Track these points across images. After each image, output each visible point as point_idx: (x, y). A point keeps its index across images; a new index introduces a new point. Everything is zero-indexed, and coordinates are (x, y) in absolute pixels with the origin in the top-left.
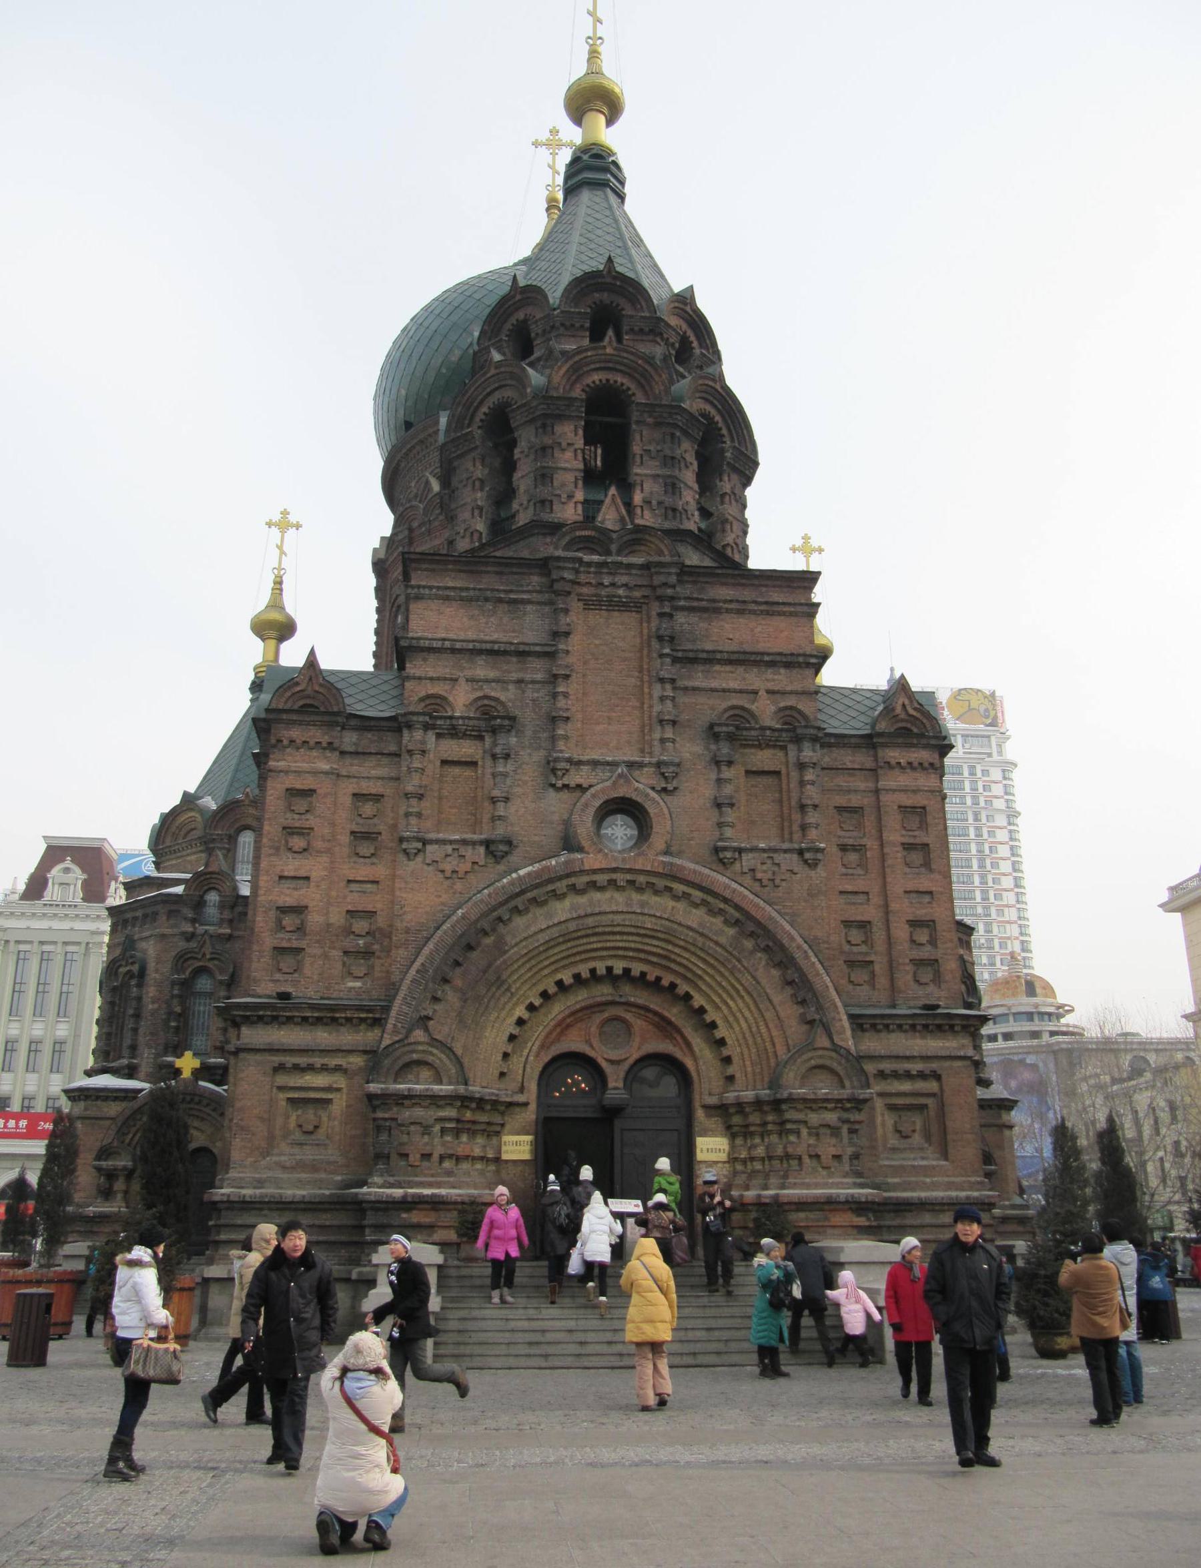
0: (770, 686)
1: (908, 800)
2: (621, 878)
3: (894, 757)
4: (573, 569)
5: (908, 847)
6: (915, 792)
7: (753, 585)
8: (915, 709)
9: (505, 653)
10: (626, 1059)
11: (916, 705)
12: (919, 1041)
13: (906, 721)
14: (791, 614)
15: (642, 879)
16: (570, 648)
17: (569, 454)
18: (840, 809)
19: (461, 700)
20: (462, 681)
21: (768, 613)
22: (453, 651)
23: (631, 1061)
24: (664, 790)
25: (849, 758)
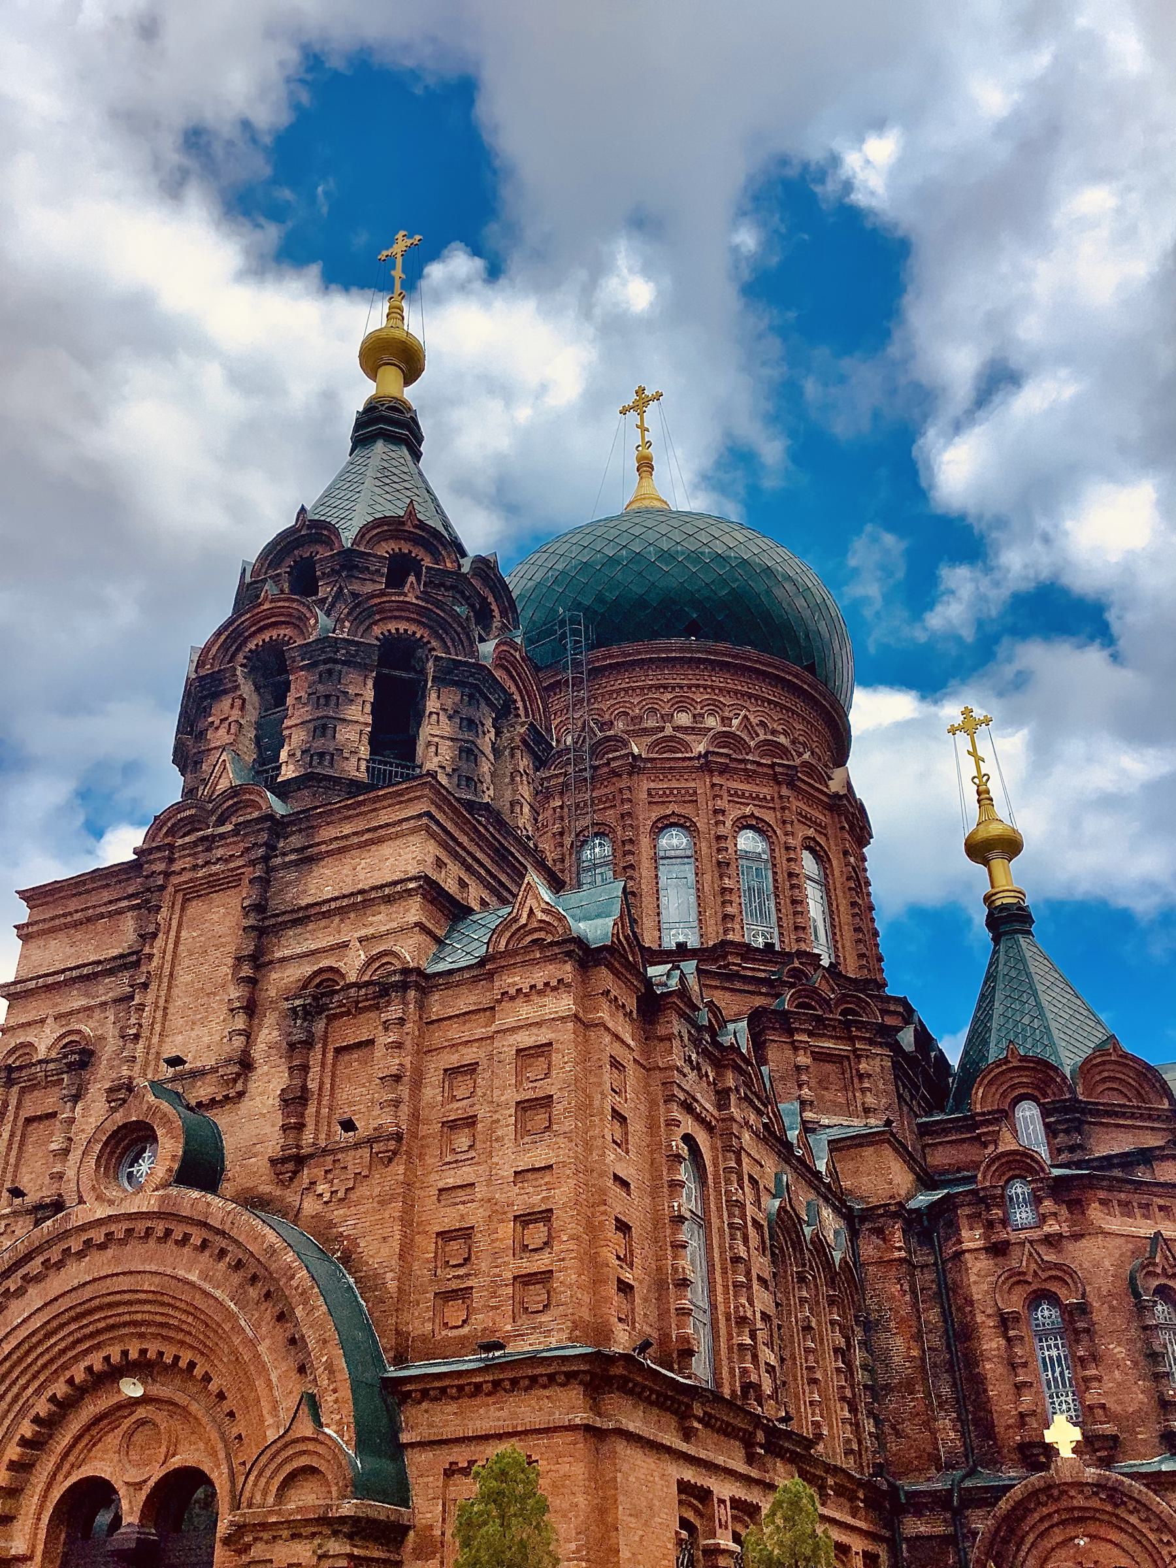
0: (363, 932)
1: (526, 1039)
2: (119, 1230)
3: (514, 984)
4: (164, 858)
5: (524, 1106)
6: (538, 1024)
7: (361, 814)
8: (543, 911)
9: (95, 975)
10: (145, 1481)
11: (543, 905)
12: (493, 1412)
13: (541, 929)
14: (398, 836)
15: (141, 1226)
16: (155, 951)
17: (222, 731)
18: (452, 1072)
19: (44, 1041)
20: (50, 1021)
21: (373, 842)
22: (48, 988)
23: (151, 1483)
24: (227, 1097)
25: (466, 1000)
